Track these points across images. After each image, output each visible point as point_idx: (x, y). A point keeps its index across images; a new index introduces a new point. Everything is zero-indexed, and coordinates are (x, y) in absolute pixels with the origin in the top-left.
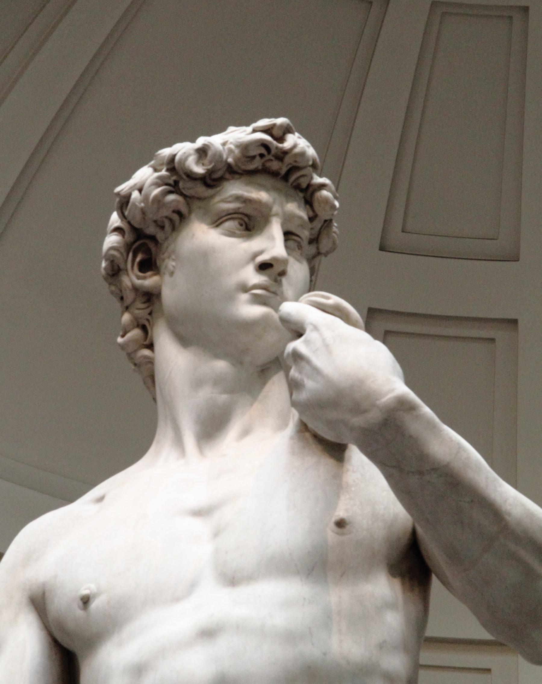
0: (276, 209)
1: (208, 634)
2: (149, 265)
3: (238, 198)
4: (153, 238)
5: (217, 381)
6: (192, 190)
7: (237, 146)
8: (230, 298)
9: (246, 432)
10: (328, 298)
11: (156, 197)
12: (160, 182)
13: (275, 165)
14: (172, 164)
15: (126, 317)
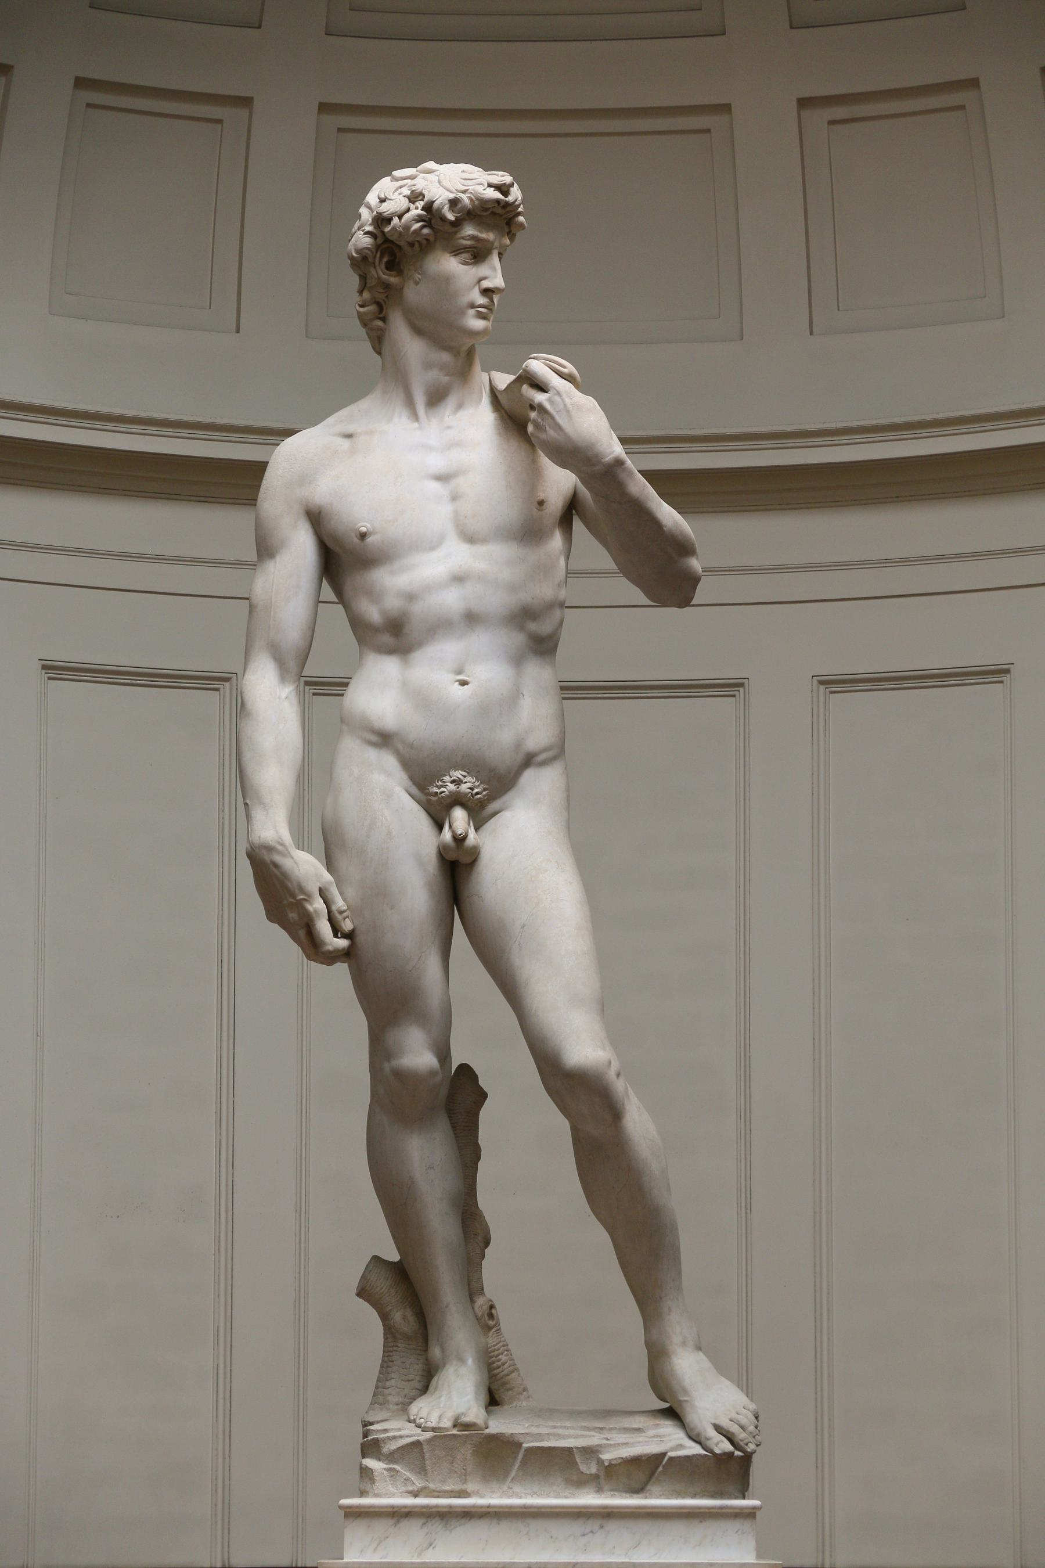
0: (496, 244)
1: (459, 579)
2: (393, 265)
3: (473, 238)
4: (399, 247)
5: (443, 367)
6: (439, 227)
7: (477, 199)
8: (462, 313)
9: (460, 406)
10: (564, 367)
11: (415, 231)
12: (419, 219)
13: (500, 211)
14: (429, 207)
15: (366, 295)
